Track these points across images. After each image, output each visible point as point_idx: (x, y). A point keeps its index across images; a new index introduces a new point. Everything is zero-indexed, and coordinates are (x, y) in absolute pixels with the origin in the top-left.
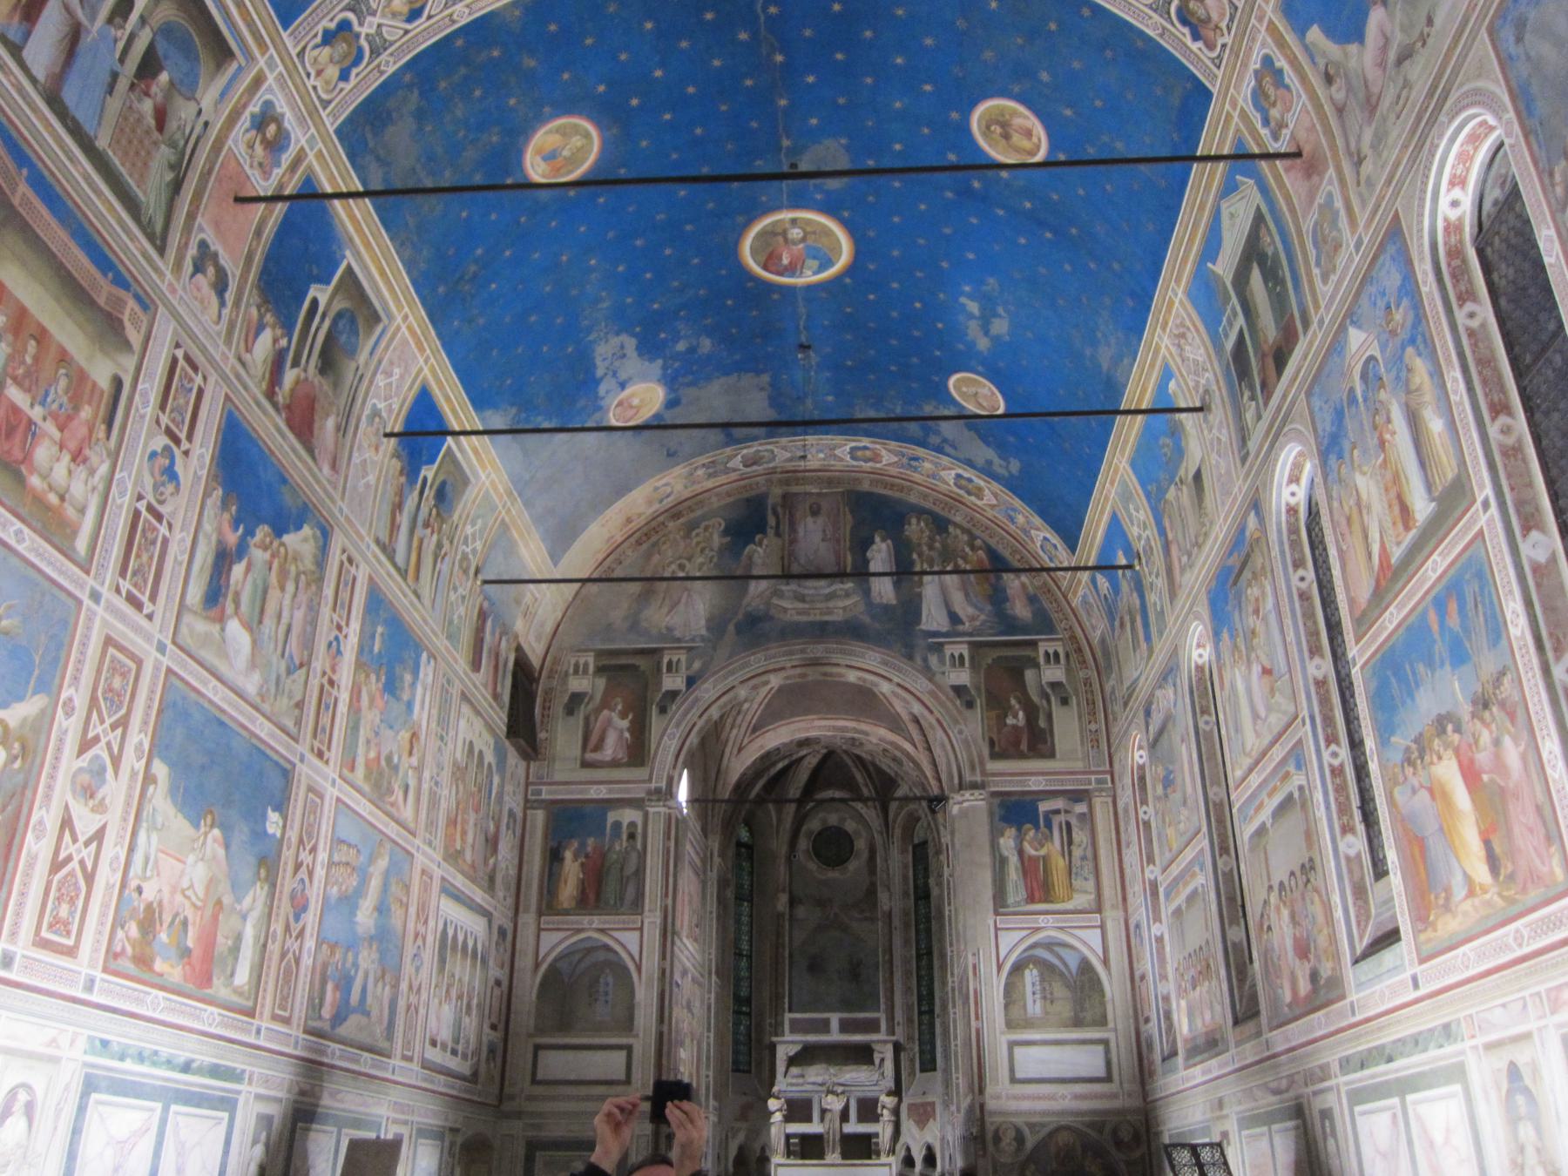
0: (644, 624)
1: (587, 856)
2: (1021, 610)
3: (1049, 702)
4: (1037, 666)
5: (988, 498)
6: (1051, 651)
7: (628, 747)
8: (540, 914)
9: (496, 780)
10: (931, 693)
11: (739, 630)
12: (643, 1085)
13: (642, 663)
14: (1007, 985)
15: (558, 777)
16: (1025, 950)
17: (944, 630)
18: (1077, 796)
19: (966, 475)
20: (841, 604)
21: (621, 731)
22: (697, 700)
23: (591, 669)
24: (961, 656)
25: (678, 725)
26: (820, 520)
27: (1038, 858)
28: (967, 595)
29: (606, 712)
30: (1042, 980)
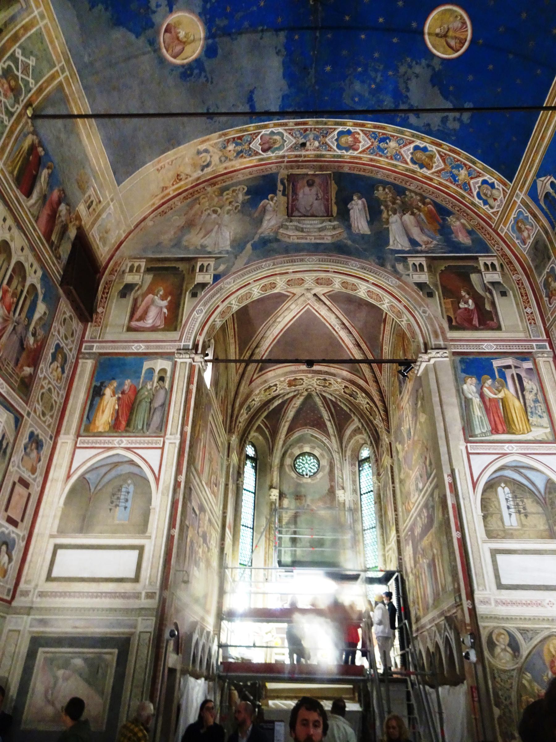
0: (184, 243)
1: (123, 393)
2: (464, 239)
3: (491, 293)
4: (479, 272)
5: (438, 164)
6: (489, 263)
7: (165, 318)
8: (78, 435)
9: (41, 308)
10: (399, 287)
11: (255, 247)
12: (150, 583)
13: (181, 266)
14: (482, 499)
15: (108, 337)
16: (495, 472)
17: (408, 249)
18: (524, 356)
19: (422, 144)
20: (329, 233)
21: (161, 308)
22: (221, 289)
23: (142, 270)
24: (421, 265)
25: (205, 304)
26: (314, 190)
27: (496, 400)
28: (422, 230)
29: (151, 296)
30: (515, 497)
